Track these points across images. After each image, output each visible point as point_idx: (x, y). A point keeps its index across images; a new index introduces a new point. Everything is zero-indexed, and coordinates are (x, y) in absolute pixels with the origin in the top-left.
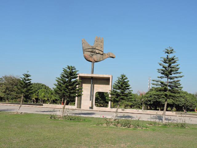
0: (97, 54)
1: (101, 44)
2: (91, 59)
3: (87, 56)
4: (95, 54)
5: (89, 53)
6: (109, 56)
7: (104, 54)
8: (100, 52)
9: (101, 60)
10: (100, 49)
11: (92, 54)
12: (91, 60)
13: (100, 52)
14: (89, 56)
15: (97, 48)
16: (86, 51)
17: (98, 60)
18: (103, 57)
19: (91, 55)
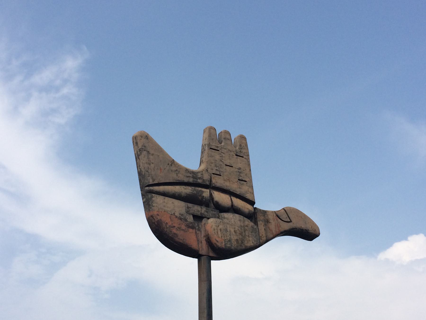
0: (226, 215)
1: (239, 163)
2: (191, 239)
3: (166, 219)
4: (212, 211)
6: (286, 227)
7: (260, 217)
8: (238, 203)
9: (251, 244)
10: (234, 187)
12: (193, 243)
13: (238, 203)
14: (176, 223)
15: (218, 181)
16: (164, 194)
17: (234, 245)
18: (255, 231)
19: (190, 219)
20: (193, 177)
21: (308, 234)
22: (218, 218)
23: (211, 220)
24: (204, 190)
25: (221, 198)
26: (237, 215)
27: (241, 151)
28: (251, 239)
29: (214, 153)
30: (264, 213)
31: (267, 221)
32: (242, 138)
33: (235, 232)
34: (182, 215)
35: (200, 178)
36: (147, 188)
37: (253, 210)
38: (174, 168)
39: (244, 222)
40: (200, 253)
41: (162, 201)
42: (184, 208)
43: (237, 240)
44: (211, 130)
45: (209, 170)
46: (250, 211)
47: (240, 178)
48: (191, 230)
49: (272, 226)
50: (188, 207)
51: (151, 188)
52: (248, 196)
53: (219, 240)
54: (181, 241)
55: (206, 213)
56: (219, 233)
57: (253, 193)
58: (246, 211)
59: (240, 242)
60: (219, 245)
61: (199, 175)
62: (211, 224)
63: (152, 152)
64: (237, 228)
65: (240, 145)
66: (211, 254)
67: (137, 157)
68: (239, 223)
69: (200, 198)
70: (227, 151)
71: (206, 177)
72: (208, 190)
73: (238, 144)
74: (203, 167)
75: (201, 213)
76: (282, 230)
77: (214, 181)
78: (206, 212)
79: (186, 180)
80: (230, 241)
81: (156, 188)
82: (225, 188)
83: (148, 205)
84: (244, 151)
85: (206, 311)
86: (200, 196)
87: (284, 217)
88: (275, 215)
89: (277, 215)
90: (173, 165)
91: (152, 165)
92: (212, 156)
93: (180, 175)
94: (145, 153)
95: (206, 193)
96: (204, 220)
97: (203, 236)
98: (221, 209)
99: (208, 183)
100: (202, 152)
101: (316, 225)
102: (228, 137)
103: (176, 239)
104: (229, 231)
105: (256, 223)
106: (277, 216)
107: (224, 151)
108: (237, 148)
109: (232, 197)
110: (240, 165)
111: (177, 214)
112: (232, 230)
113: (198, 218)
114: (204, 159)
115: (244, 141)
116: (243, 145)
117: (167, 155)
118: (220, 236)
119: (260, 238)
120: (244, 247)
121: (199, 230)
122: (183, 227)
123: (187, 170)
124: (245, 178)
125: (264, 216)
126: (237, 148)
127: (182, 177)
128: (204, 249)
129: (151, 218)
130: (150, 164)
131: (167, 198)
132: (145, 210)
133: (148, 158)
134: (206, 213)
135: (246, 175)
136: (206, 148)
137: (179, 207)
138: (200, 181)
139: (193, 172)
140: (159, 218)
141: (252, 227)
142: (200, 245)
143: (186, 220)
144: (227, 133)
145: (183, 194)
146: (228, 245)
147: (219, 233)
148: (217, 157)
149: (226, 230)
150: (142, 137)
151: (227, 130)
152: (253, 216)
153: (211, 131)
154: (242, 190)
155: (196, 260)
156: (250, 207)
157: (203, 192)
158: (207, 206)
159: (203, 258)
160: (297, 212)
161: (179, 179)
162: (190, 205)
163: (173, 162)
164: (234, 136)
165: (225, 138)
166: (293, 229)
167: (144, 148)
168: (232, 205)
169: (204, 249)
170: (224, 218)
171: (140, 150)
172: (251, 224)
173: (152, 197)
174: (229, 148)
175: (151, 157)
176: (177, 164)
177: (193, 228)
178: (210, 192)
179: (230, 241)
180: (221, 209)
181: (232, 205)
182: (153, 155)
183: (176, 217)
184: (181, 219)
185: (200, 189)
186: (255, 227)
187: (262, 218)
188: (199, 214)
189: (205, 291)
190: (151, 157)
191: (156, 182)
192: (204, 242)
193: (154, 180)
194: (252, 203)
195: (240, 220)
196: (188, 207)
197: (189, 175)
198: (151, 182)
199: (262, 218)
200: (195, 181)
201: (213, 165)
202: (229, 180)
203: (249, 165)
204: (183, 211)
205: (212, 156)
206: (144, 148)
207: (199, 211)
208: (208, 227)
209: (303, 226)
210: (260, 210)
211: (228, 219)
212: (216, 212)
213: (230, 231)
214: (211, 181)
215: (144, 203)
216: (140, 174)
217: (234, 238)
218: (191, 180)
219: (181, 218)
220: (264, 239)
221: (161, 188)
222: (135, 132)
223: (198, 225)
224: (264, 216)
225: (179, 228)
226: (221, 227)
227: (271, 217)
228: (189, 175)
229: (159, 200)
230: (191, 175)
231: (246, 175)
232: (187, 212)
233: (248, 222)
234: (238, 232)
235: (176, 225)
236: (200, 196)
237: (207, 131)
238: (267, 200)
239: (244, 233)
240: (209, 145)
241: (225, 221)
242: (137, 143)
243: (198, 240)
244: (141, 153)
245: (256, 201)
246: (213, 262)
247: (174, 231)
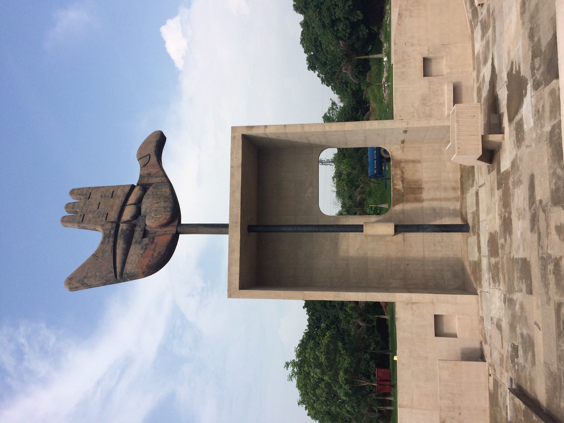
0: (143, 210)
1: (96, 197)
2: (163, 240)
4: (140, 222)
5: (133, 248)
6: (154, 159)
7: (145, 181)
8: (133, 199)
9: (168, 190)
10: (118, 202)
12: (167, 238)
13: (133, 199)
15: (113, 216)
16: (124, 263)
17: (169, 204)
19: (146, 240)
20: (109, 238)
21: (160, 141)
22: (145, 216)
23: (147, 223)
24: (120, 229)
26: (143, 201)
27: (85, 194)
28: (164, 190)
29: (86, 219)
30: (141, 177)
31: (149, 175)
32: (72, 192)
33: (157, 203)
34: (142, 248)
35: (110, 232)
36: (118, 278)
37: (139, 187)
38: (101, 254)
39: (149, 195)
40: (174, 232)
41: (130, 265)
42: (137, 246)
43: (165, 202)
44: (65, 221)
45: (102, 223)
46: (140, 190)
47: (110, 196)
48: (156, 240)
49: (153, 171)
50: (136, 242)
51: (118, 274)
52: (127, 190)
53: (165, 216)
54: (165, 249)
55: (141, 227)
56: (158, 216)
57: (124, 186)
59: (166, 199)
60: (168, 217)
61: (107, 232)
62: (150, 223)
63: (85, 274)
64: (154, 201)
65: (80, 194)
66: (176, 223)
67: (90, 286)
68: (151, 199)
69: (127, 232)
70: (84, 207)
71: (109, 226)
72: (121, 224)
73: (79, 196)
74: (99, 228)
75: (141, 231)
76: (156, 163)
77: (113, 220)
78: (140, 226)
79: (111, 244)
80: (165, 208)
81: (118, 270)
82: (119, 210)
83: (133, 277)
84: (84, 193)
85: (221, 229)
86: (126, 232)
87: (145, 160)
88: (144, 168)
89: (143, 166)
90: (98, 255)
91: (97, 273)
92: (90, 221)
93: (107, 249)
94: (85, 281)
95: (123, 226)
96: (147, 229)
97: (160, 230)
98: (138, 214)
99: (114, 225)
100: (86, 229)
101: (153, 134)
102: (71, 205)
103: (163, 252)
104: (155, 209)
105: (151, 185)
106: (145, 166)
108: (82, 197)
109: (128, 204)
110: (99, 196)
111: (141, 252)
112: (156, 205)
113: (145, 233)
114: (92, 228)
115: (76, 191)
116: (79, 192)
117: (88, 260)
118: (161, 216)
119: (163, 182)
120: (171, 196)
121: (155, 233)
122: (153, 246)
123: (102, 243)
124: (111, 192)
125: (144, 177)
126: (82, 197)
127: (109, 248)
128: (171, 230)
129: (145, 273)
130: (96, 276)
131: (127, 261)
132: (138, 278)
133: (90, 277)
134: (141, 227)
135: (107, 191)
136: (82, 225)
137: (135, 251)
138: (112, 232)
139: (104, 238)
140: (144, 267)
141: (154, 188)
142: (168, 233)
143: (147, 244)
144: (67, 206)
145: (124, 246)
146: (169, 209)
147: (158, 216)
148: (90, 216)
149: (156, 210)
150: (70, 284)
151: (64, 206)
152: (144, 187)
153: (65, 221)
154: (121, 195)
155: (180, 235)
157: (122, 229)
158: (135, 225)
159: (179, 230)
160: (141, 148)
161: (110, 250)
162: (134, 240)
163: (94, 255)
164: (71, 200)
165: (73, 208)
166: (156, 154)
167: (80, 280)
168: (135, 204)
169: (171, 230)
170: (145, 212)
171: (83, 285)
172: (151, 188)
173: (126, 273)
174: (82, 205)
175: (89, 275)
176: (96, 252)
177: (153, 238)
178: (122, 223)
179: (165, 208)
180: (138, 214)
181: (135, 204)
182: (87, 273)
183: (144, 252)
184: (146, 249)
185: (119, 232)
186: (154, 185)
187: (146, 179)
188: (142, 233)
189: (206, 229)
190: (89, 275)
191: (113, 270)
192: (166, 229)
193: (111, 272)
194: (133, 187)
195: (148, 198)
196: (136, 242)
197: (106, 241)
198: (113, 274)
199: (146, 179)
200: (112, 236)
201: (98, 220)
202: (112, 206)
203: (98, 188)
204: (139, 246)
205: (90, 221)
206: (80, 280)
207: (139, 233)
208: (154, 226)
209: (154, 144)
210: (139, 180)
211: (146, 209)
212: (140, 218)
213: (157, 207)
214: (112, 222)
215: (131, 280)
216: (105, 284)
217: (163, 204)
218: (112, 239)
220: (164, 179)
221: (119, 265)
222: (66, 290)
223: (152, 234)
224: (144, 177)
225: (154, 250)
226: (153, 215)
227: (146, 172)
228: (106, 241)
229: (129, 268)
230: (107, 239)
231: (107, 191)
232: (140, 243)
233: (149, 192)
234: (157, 200)
235: (151, 252)
236: (126, 232)
237: (65, 224)
238: (130, 174)
239: (159, 196)
240: (78, 223)
241: (148, 211)
242: (76, 288)
243: (164, 234)
244: (86, 284)
245: (131, 183)
246: (183, 222)
247: (156, 254)
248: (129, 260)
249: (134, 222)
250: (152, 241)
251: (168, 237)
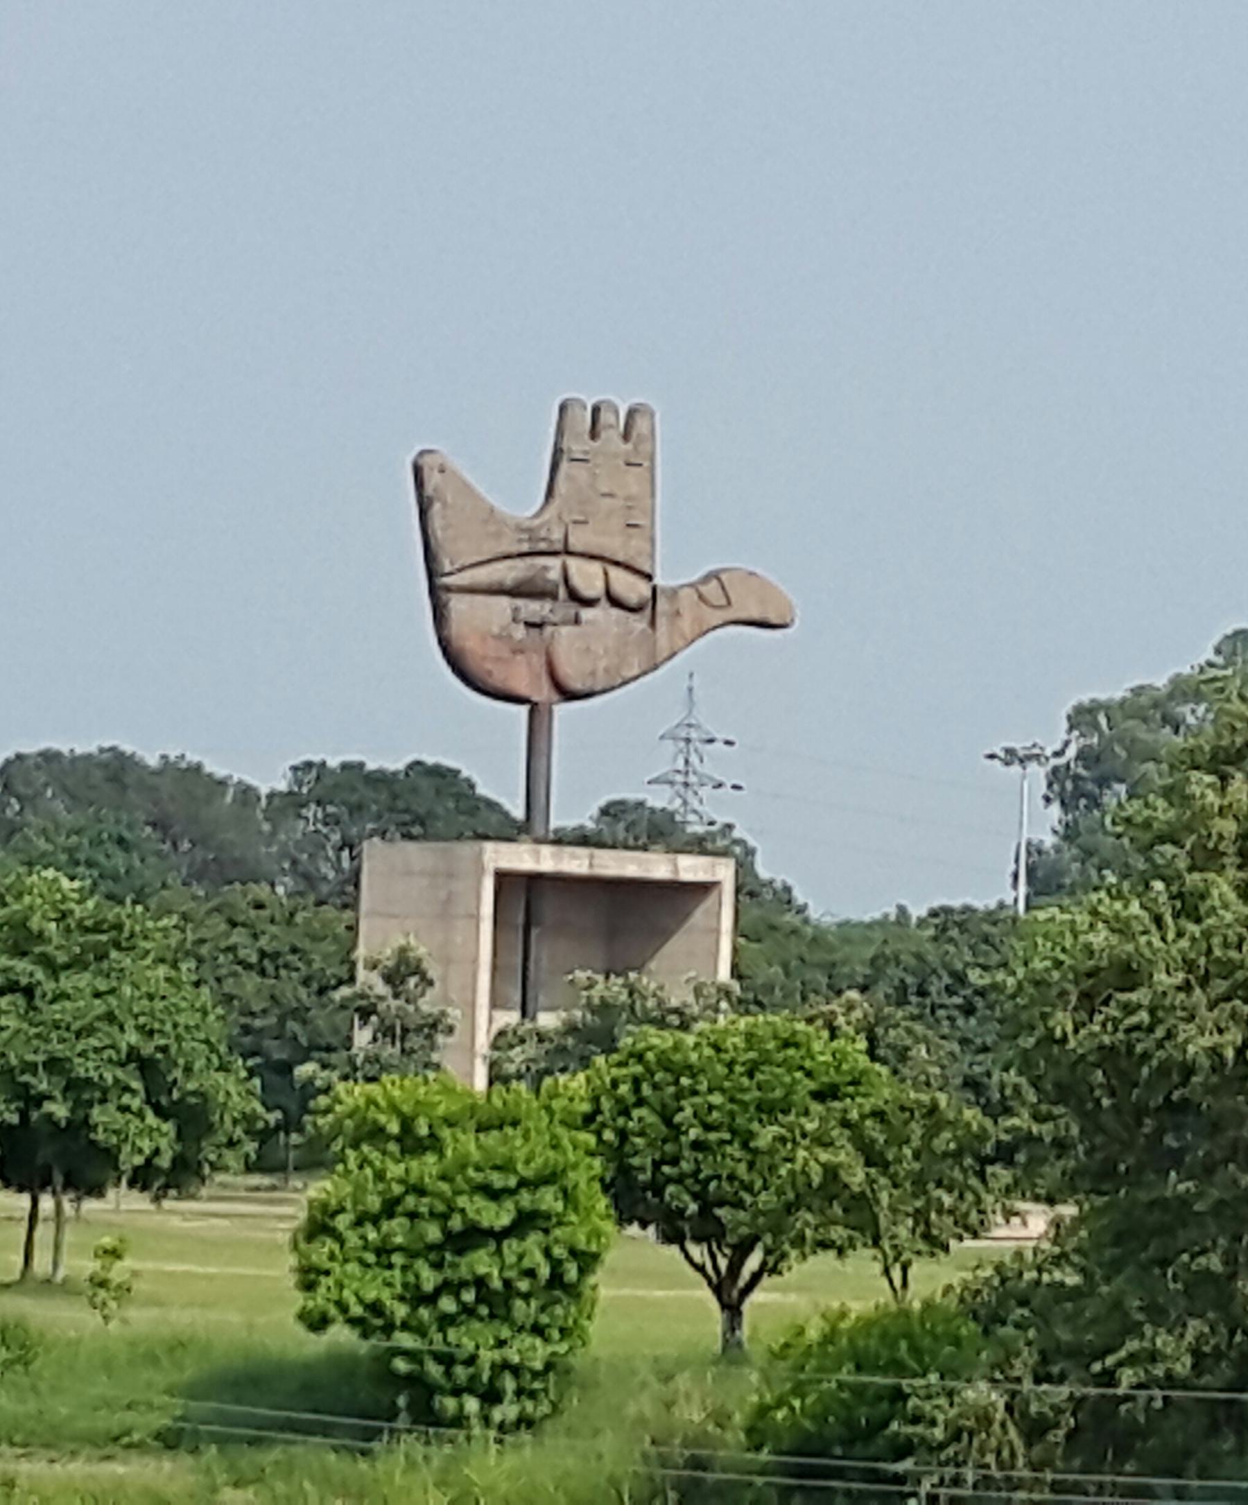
0: (586, 614)
1: (632, 482)
5: (505, 602)
10: (615, 546)
11: (533, 608)
14: (492, 649)
19: (520, 632)
20: (530, 539)
25: (588, 578)
35: (544, 539)
58: (632, 599)
79: (515, 549)
96: (548, 630)
99: (559, 546)
107: (599, 460)
110: (634, 489)
119: (653, 653)
122: (506, 654)
156: (644, 589)
162: (520, 602)
188: (537, 620)
194: (649, 577)
218: (525, 547)
219: (503, 637)
232: (515, 620)
248: (480, 599)
249: (562, 592)
250: (518, 650)
251: (522, 689)
